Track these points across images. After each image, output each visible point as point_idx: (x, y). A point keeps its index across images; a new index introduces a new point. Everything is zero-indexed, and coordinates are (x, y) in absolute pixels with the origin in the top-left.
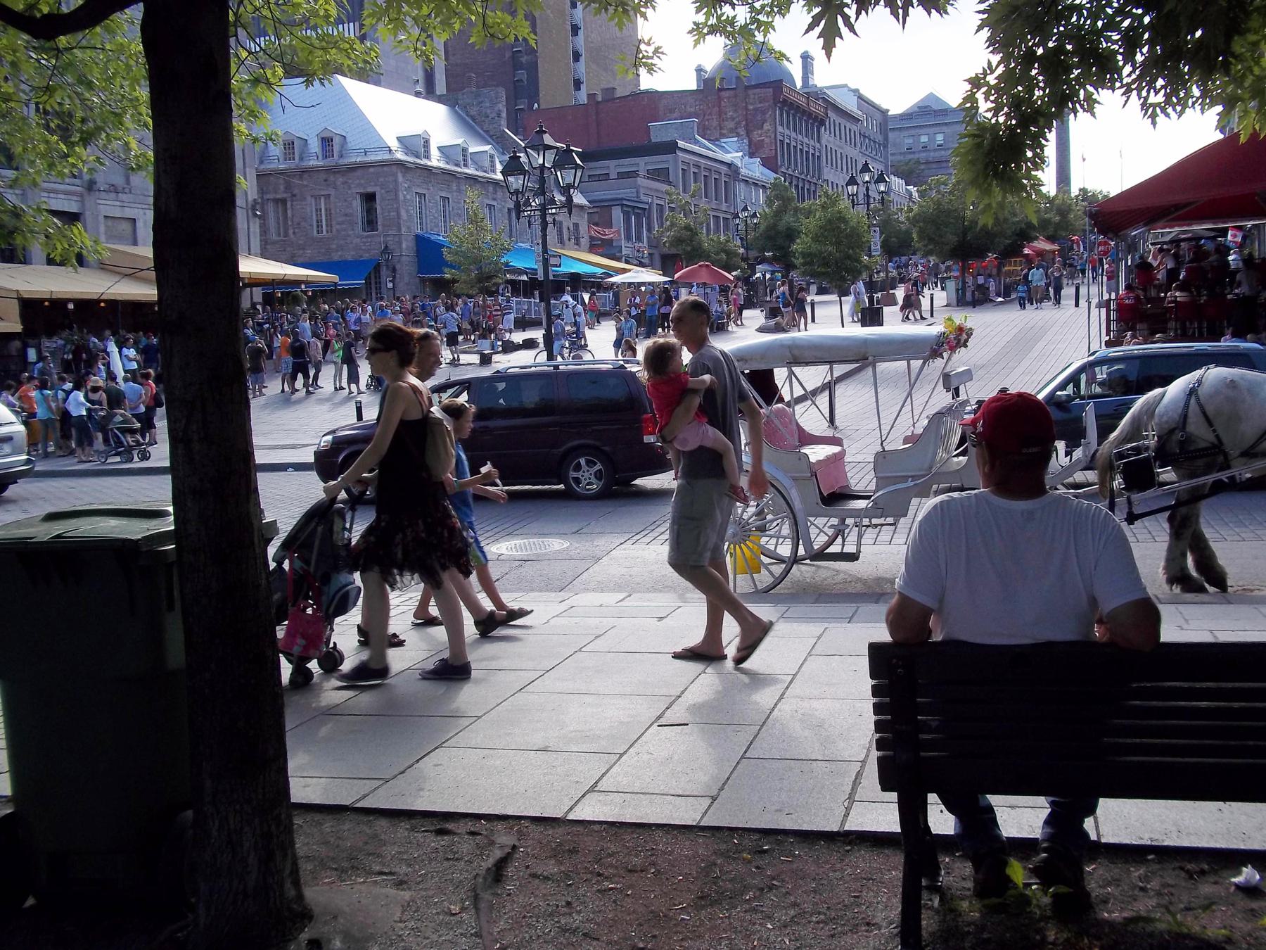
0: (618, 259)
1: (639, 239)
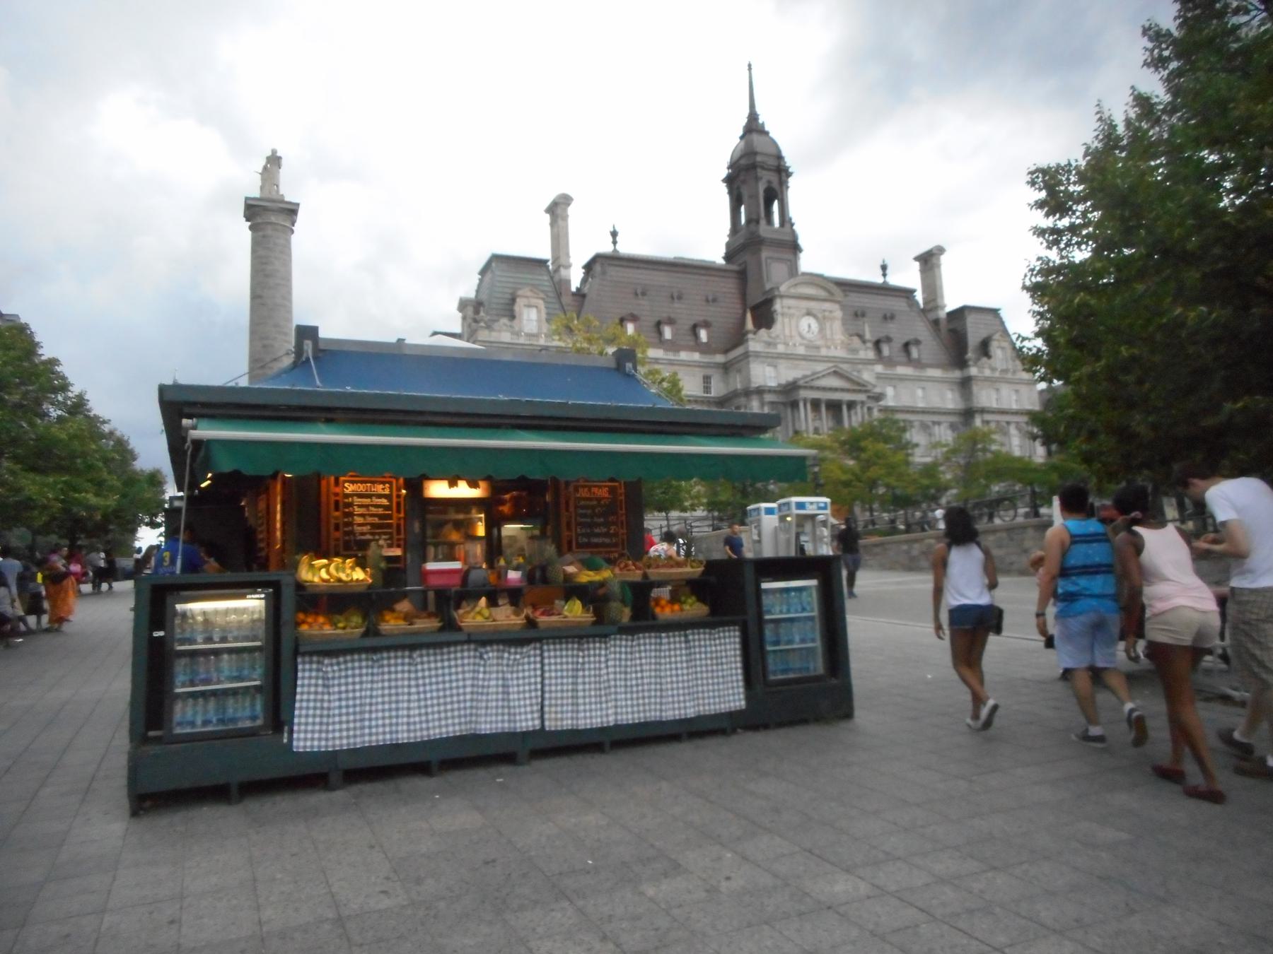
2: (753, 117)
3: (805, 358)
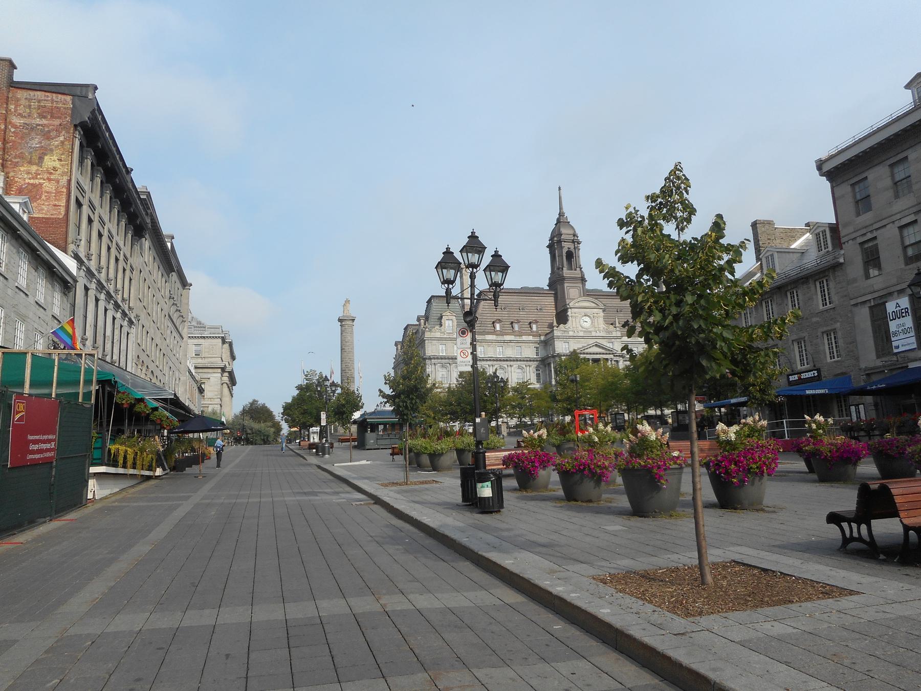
2: (561, 214)
3: (583, 337)
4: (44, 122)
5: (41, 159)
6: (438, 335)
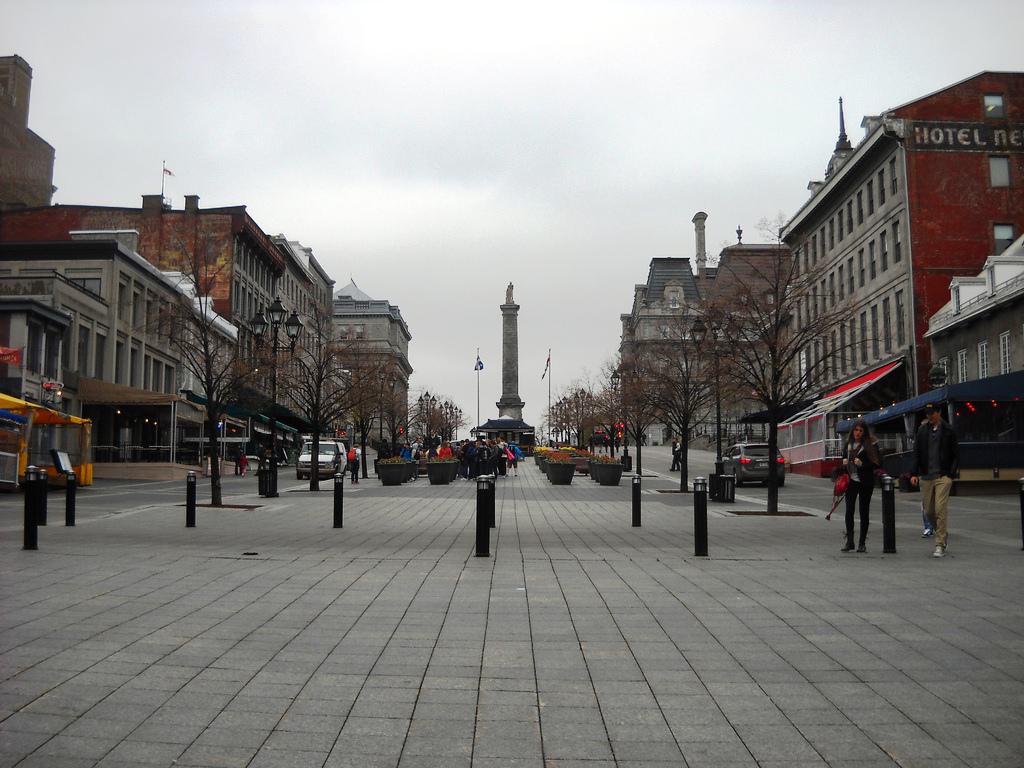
0: (18, 396)
1: (50, 372)
4: (216, 234)
5: (215, 261)
6: (658, 312)
